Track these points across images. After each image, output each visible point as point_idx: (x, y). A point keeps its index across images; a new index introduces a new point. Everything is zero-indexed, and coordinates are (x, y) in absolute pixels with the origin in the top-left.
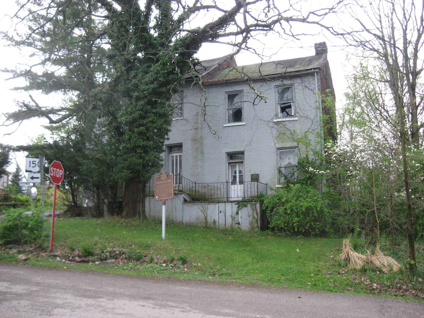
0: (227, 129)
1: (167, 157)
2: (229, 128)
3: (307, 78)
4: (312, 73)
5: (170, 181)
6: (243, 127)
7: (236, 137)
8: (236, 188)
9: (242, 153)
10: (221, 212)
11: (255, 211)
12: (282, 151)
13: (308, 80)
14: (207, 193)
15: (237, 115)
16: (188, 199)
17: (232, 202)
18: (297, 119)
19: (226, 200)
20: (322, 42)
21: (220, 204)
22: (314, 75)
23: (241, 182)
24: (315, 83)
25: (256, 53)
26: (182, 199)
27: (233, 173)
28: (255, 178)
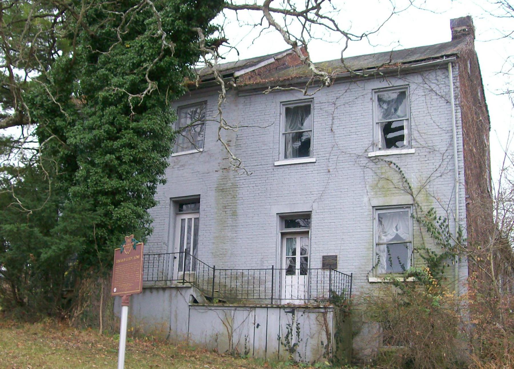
0: (281, 170)
1: (172, 220)
2: (286, 169)
3: (434, 74)
4: (442, 65)
5: (138, 257)
6: (310, 167)
7: (296, 186)
8: (295, 282)
9: (307, 216)
10: (258, 325)
11: (324, 328)
12: (383, 213)
13: (435, 80)
14: (239, 288)
15: (304, 148)
16: (199, 299)
17: (279, 307)
18: (412, 151)
19: (268, 302)
20: (465, 15)
21: (257, 310)
22: (447, 69)
23: (304, 271)
24: (450, 82)
25: (338, 30)
26: (189, 299)
27: (291, 253)
28: (330, 263)
